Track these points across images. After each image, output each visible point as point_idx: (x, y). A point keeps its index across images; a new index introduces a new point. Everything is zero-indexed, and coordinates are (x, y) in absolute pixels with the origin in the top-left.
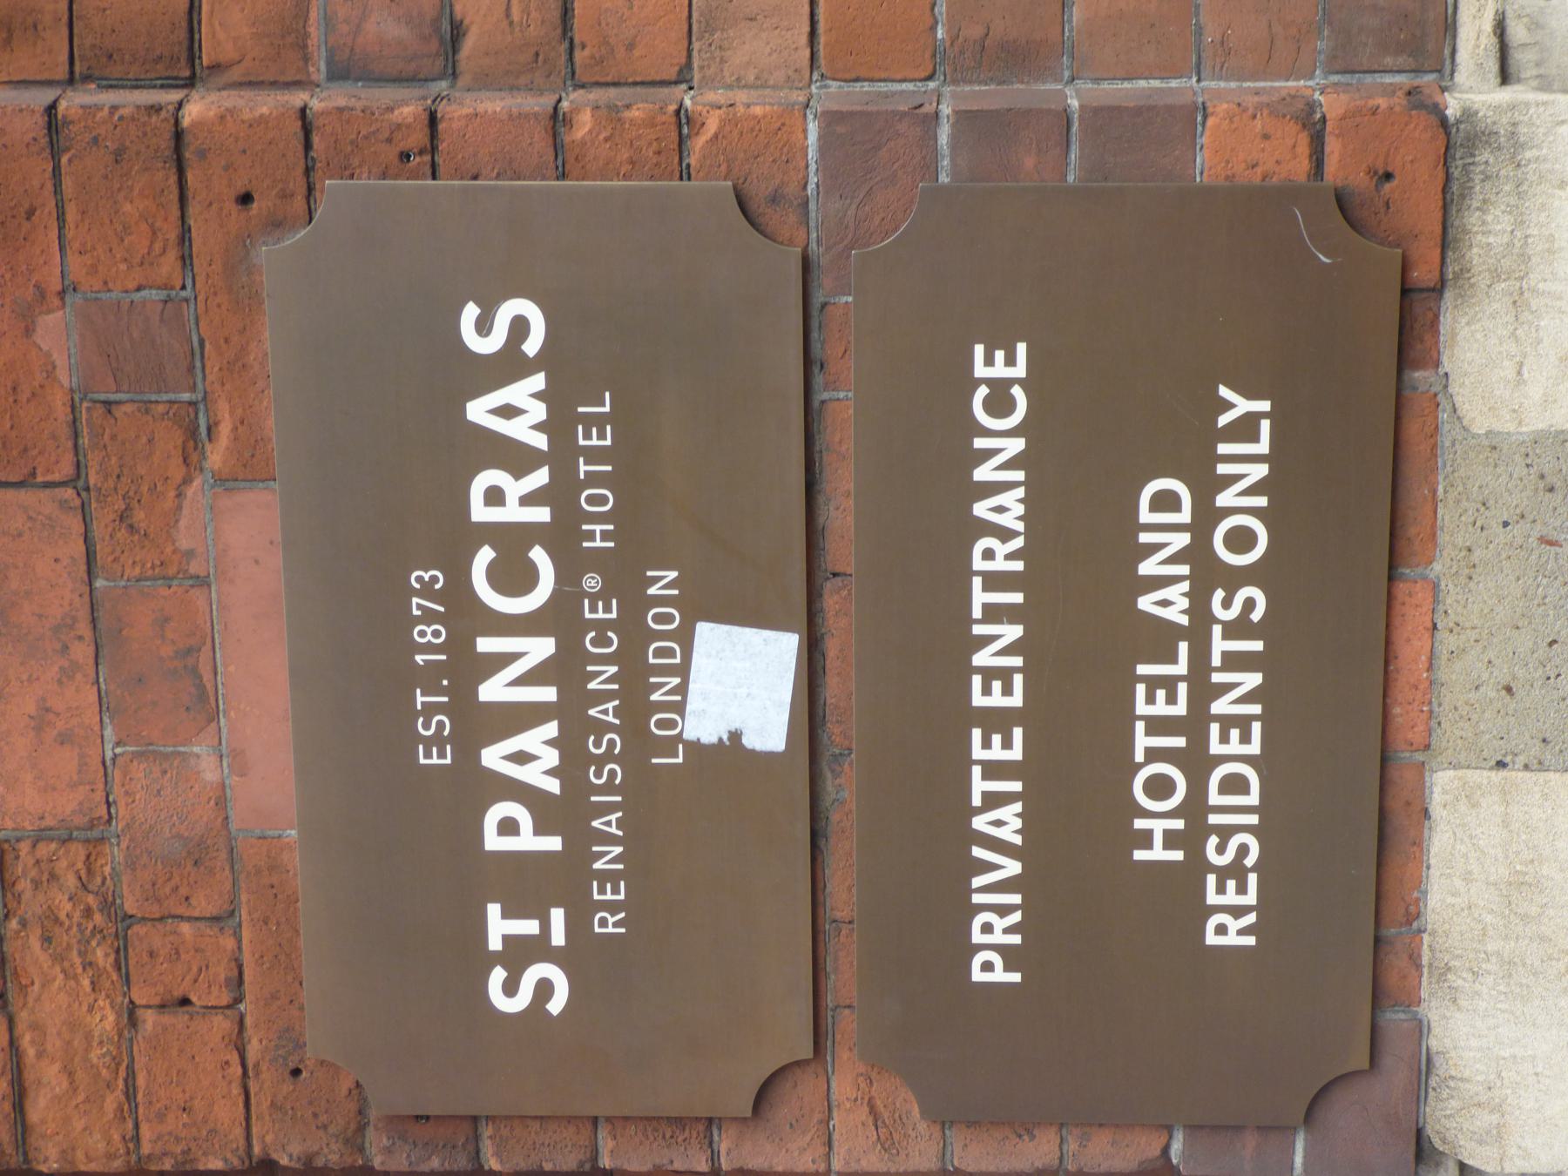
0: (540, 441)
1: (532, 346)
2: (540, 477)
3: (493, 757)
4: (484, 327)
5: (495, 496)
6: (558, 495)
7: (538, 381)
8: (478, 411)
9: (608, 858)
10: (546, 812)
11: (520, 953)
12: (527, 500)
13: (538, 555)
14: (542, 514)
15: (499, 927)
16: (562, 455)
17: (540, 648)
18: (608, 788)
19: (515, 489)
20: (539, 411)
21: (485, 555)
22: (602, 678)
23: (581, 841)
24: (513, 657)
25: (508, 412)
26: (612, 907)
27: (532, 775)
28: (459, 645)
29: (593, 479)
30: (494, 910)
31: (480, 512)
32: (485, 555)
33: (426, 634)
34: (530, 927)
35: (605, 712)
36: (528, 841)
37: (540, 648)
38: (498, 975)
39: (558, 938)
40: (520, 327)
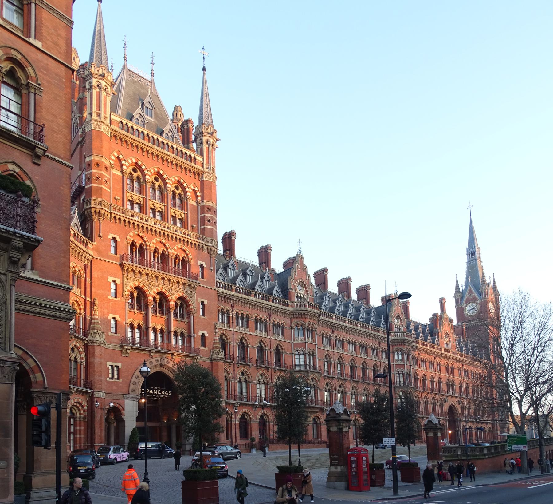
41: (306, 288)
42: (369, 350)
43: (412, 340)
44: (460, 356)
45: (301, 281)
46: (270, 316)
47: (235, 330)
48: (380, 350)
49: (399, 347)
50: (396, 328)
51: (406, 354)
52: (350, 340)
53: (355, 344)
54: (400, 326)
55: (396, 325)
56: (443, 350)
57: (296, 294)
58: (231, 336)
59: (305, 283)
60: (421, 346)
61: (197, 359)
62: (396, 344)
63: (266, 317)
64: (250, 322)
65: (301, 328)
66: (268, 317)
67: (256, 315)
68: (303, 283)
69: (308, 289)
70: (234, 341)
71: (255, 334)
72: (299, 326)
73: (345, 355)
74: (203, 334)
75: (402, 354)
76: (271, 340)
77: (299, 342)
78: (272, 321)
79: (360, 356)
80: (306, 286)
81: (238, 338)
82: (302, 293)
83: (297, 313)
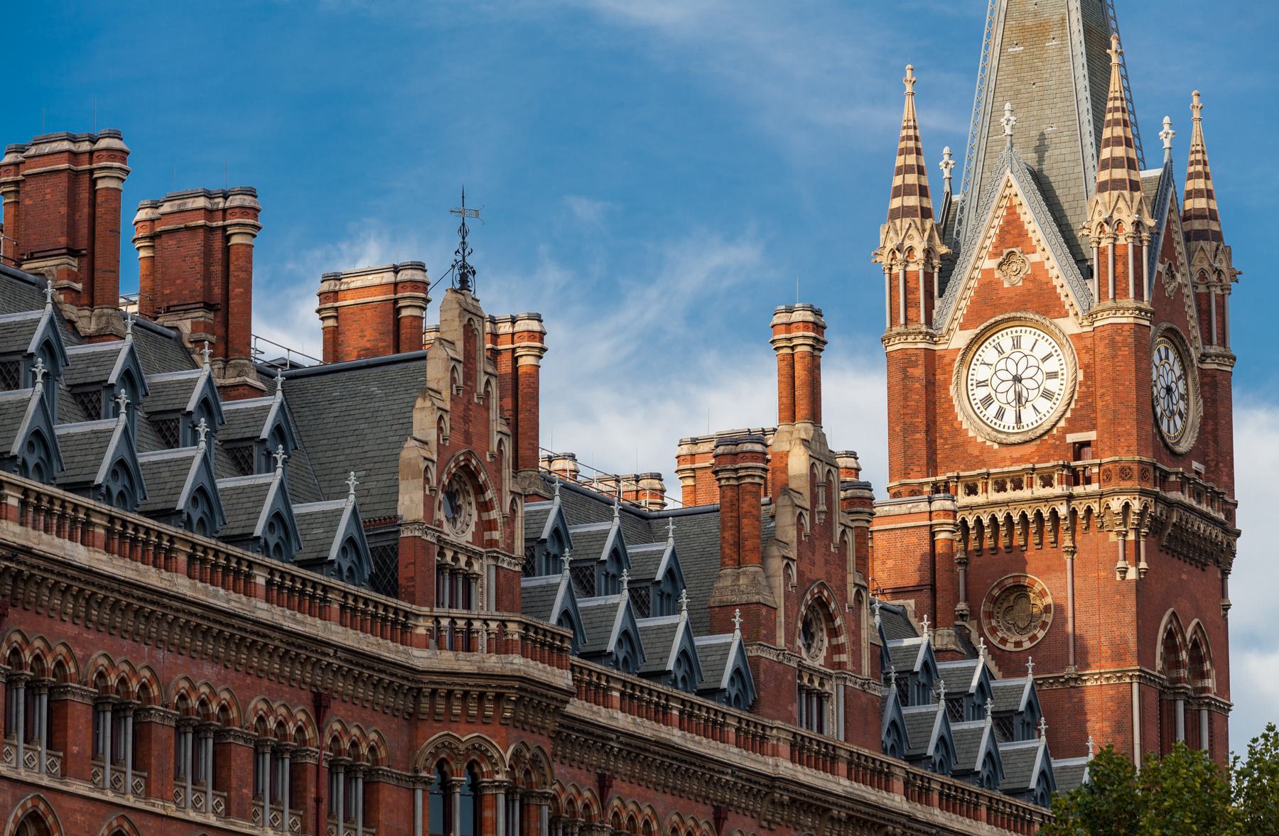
42: (241, 756)
43: (563, 679)
44: (908, 796)
48: (317, 752)
49: (468, 736)
50: (441, 568)
51: (510, 792)
52: (113, 680)
53: (140, 713)
54: (472, 556)
55: (443, 544)
56: (785, 749)
60: (623, 721)
62: (441, 707)
73: (67, 803)
75: (475, 787)
79: (172, 810)
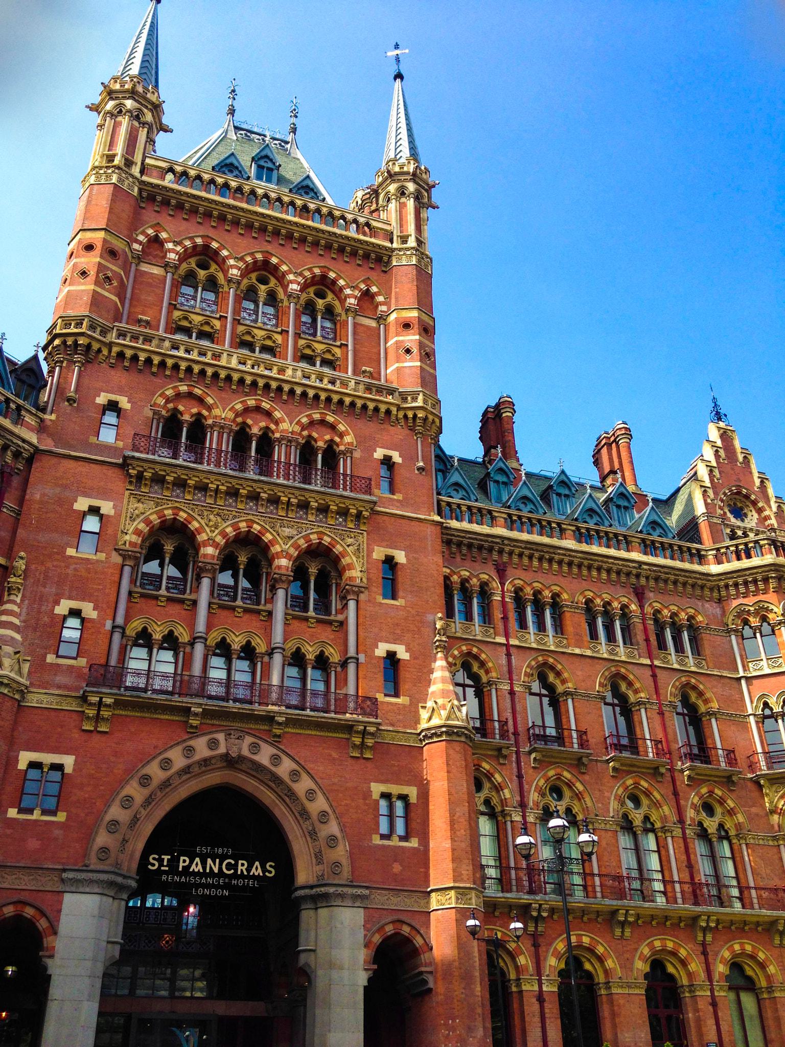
0: (251, 874)
1: (267, 874)
2: (245, 873)
3: (197, 860)
4: (271, 866)
5: (243, 865)
6: (242, 876)
7: (261, 874)
8: (257, 863)
9: (177, 879)
10: (186, 868)
11: (161, 861)
12: (242, 870)
13: (232, 871)
14: (239, 873)
15: (166, 858)
16: (249, 877)
17: (216, 870)
18: (190, 880)
19: (244, 868)
20: (256, 874)
21: (233, 862)
22: (210, 881)
23: (180, 874)
24: (215, 865)
25: (257, 868)
26: (167, 879)
27: (194, 866)
28: (217, 856)
29: (244, 881)
30: (169, 857)
31: (240, 862)
32: (233, 862)
33: (220, 851)
34: (165, 863)
35: (203, 880)
36: (181, 864)
37: (216, 870)
38: (157, 857)
39: (162, 868)
40: (270, 872)
41: (760, 511)
45: (739, 493)
46: (640, 595)
47: (513, 642)
57: (728, 531)
58: (503, 661)
59: (753, 497)
61: (364, 733)
63: (625, 600)
64: (567, 615)
65: (766, 628)
66: (635, 600)
67: (590, 595)
68: (747, 497)
69: (767, 513)
70: (515, 677)
71: (589, 653)
72: (754, 621)
74: (391, 655)
76: (658, 671)
77: (767, 671)
78: (648, 610)
80: (760, 505)
81: (524, 666)
82: (749, 526)
83: (740, 581)
